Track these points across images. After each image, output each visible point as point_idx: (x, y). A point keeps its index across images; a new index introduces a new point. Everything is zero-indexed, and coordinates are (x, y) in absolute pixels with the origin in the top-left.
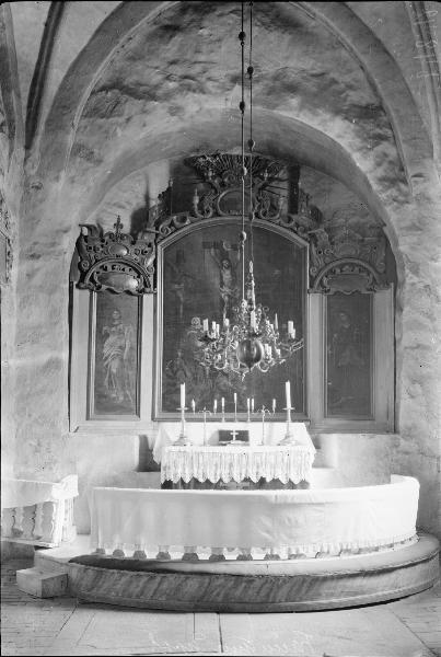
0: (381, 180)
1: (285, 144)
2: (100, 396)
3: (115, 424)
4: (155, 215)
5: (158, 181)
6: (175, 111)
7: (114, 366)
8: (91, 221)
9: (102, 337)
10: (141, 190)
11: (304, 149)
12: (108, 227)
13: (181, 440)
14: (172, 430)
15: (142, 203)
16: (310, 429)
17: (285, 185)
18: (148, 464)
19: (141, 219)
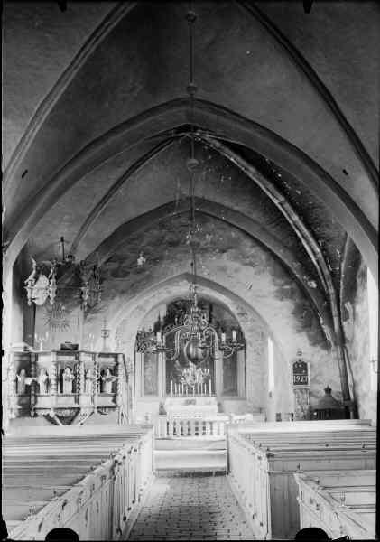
0: (238, 314)
1: (205, 297)
2: (145, 388)
3: (153, 398)
4: (162, 325)
5: (163, 312)
6: (169, 292)
7: (149, 379)
8: (141, 329)
9: (145, 368)
10: (157, 316)
11: (212, 301)
12: (147, 331)
13: (171, 404)
14: (168, 400)
15: (156, 320)
16: (217, 399)
17: (207, 311)
18: (162, 413)
19: (157, 327)
